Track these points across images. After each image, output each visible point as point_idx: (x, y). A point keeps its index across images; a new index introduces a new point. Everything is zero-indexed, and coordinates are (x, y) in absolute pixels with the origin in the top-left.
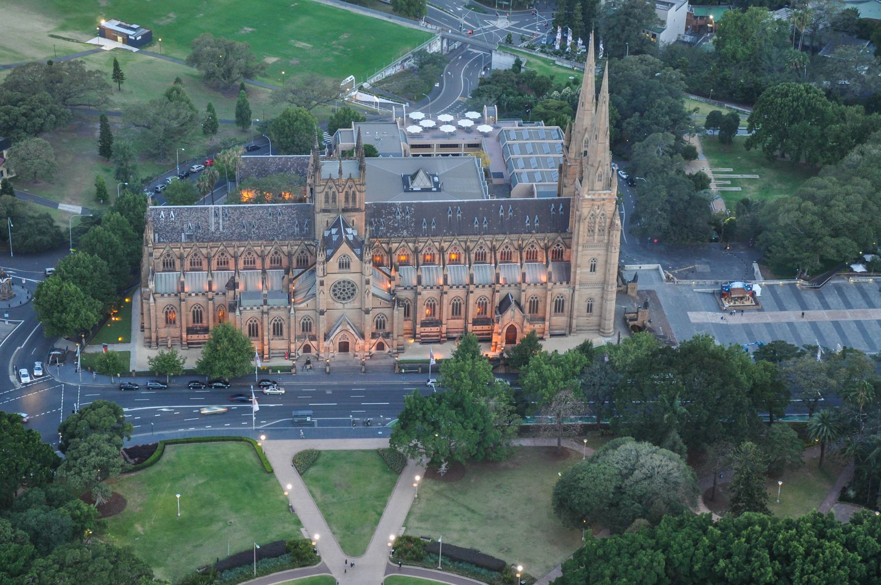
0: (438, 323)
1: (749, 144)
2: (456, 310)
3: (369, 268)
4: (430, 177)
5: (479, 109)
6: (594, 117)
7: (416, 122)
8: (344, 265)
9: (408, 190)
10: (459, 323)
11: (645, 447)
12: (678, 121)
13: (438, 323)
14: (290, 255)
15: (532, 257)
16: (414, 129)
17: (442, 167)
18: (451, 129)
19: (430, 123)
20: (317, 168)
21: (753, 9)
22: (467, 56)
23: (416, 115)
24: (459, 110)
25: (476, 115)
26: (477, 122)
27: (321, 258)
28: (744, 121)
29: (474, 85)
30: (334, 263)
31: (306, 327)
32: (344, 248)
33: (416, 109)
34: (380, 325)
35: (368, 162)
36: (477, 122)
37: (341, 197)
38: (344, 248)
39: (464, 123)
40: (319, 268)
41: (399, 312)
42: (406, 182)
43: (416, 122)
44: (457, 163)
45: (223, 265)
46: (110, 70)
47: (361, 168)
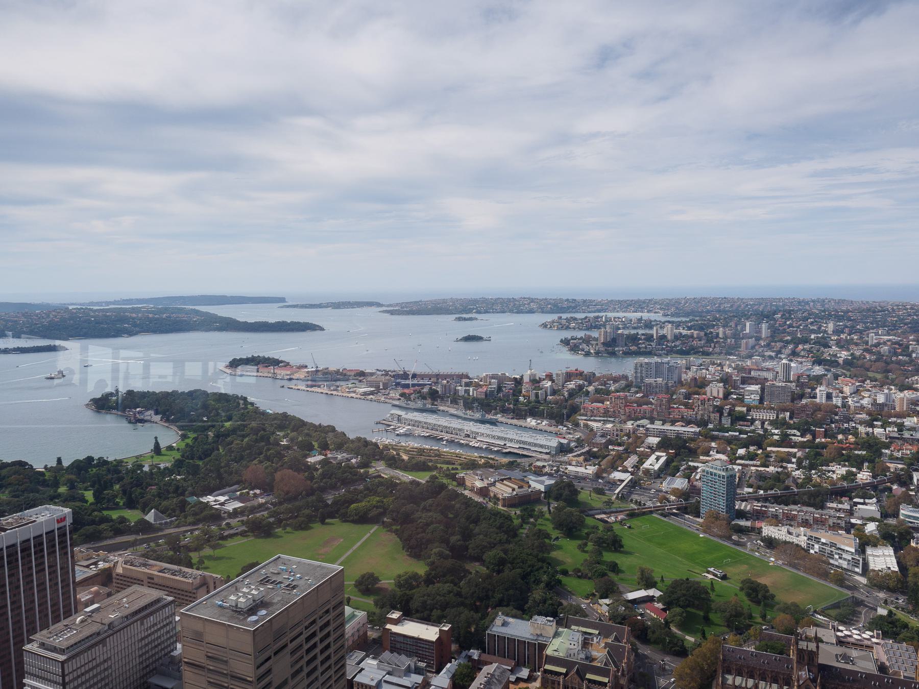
7: (842, 631)
16: (839, 634)
17: (854, 653)
18: (859, 638)
20: (797, 644)
24: (861, 630)
26: (872, 637)
29: (868, 620)
35: (820, 644)
36: (872, 637)
43: (842, 631)
45: (752, 677)
46: (709, 586)
47: (818, 647)
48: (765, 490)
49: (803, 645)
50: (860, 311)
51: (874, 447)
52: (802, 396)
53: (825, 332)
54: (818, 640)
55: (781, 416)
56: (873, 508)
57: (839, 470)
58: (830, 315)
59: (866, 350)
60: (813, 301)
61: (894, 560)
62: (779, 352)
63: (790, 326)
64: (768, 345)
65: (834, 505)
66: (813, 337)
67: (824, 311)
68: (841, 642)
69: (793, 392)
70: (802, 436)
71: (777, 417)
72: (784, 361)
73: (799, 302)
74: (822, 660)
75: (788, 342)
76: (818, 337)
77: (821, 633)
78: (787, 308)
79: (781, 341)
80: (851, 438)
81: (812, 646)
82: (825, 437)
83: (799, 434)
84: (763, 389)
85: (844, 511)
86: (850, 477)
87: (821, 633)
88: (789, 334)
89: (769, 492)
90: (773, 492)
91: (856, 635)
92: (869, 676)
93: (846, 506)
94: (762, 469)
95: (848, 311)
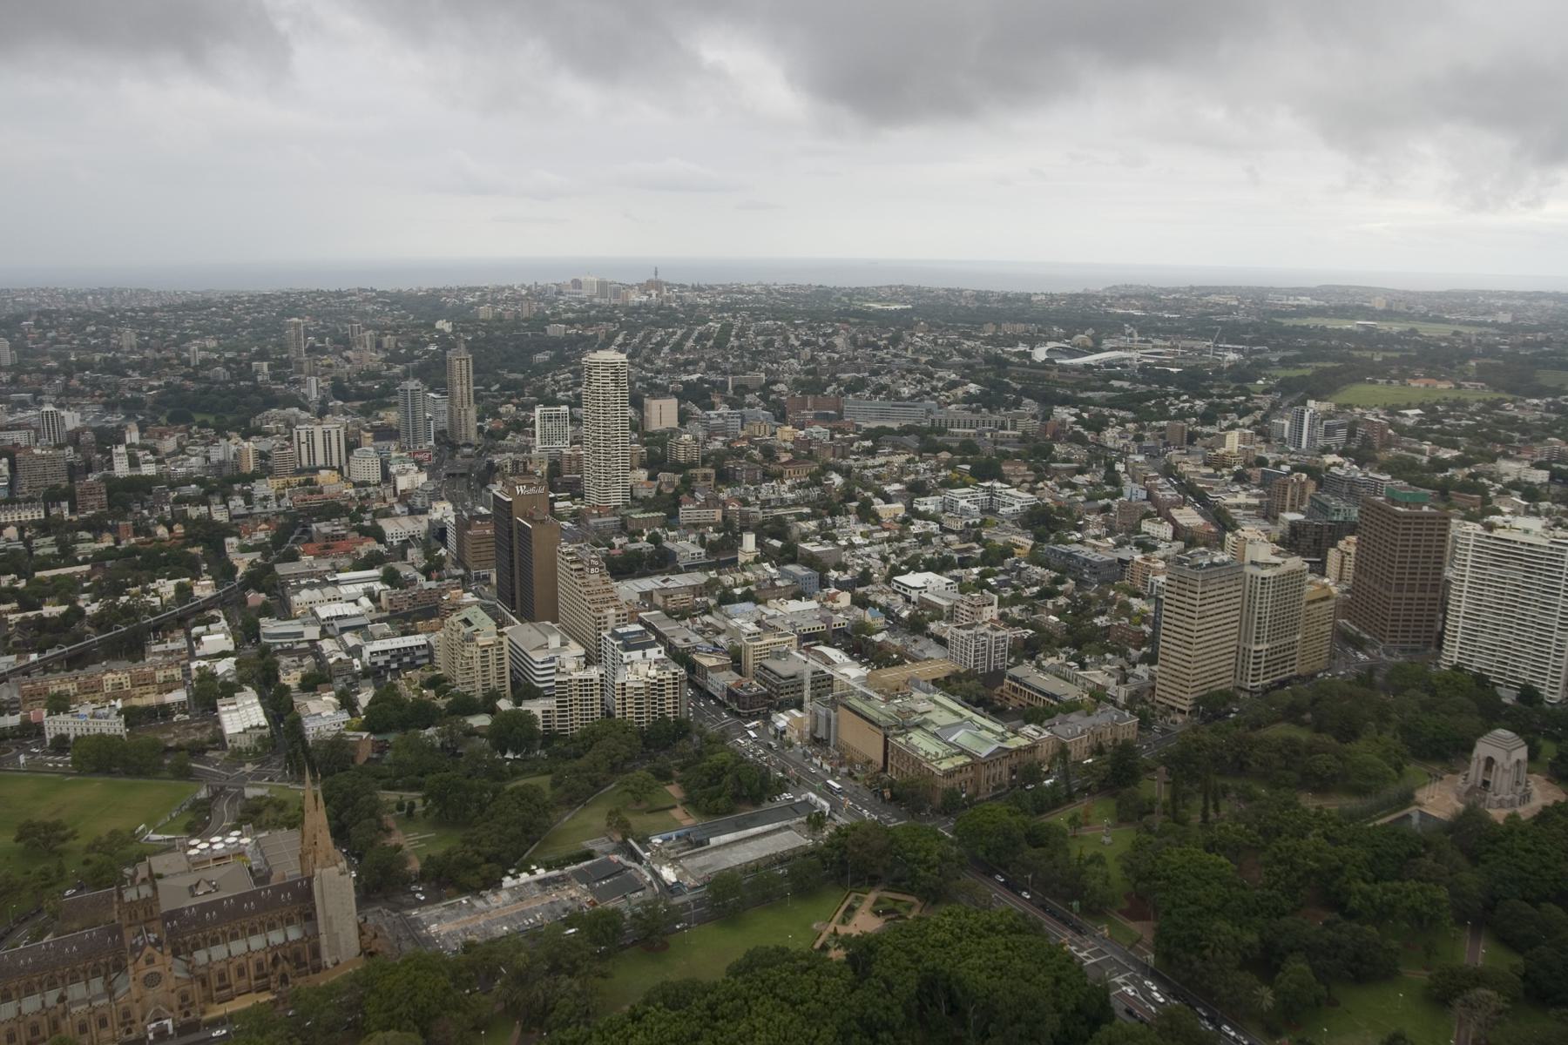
0: (229, 986)
1: (425, 814)
2: (241, 972)
3: (169, 959)
4: (209, 883)
5: (239, 829)
6: (318, 819)
7: (194, 847)
8: (150, 961)
9: (193, 896)
10: (244, 981)
11: (392, 1033)
12: (375, 810)
13: (229, 986)
14: (107, 964)
15: (290, 922)
16: (192, 852)
17: (215, 874)
19: (205, 845)
20: (121, 896)
21: (411, 731)
22: (227, 794)
23: (194, 842)
24: (225, 833)
25: (237, 833)
27: (130, 961)
28: (419, 802)
30: (142, 961)
31: (126, 1014)
32: (149, 949)
33: (193, 837)
34: (184, 998)
35: (159, 882)
36: (241, 836)
37: (141, 913)
38: (149, 949)
39: (230, 840)
40: (130, 968)
41: (197, 986)
42: (192, 890)
43: (194, 847)
44: (227, 869)
47: (155, 888)
48: (41, 651)
49: (131, 895)
50: (172, 308)
51: (212, 535)
52: (89, 469)
53: (118, 349)
54: (153, 878)
55: (54, 511)
56: (222, 636)
57: (167, 587)
58: (123, 317)
59: (186, 376)
60: (92, 292)
61: (259, 709)
62: (38, 392)
63: (55, 341)
64: (14, 381)
65: (161, 647)
66: (97, 357)
67: (112, 311)
68: (199, 863)
69: (71, 466)
70: (95, 540)
71: (47, 514)
72: (48, 408)
73: (67, 295)
74: (166, 905)
75: (51, 373)
76: (106, 359)
77: (159, 863)
78: (45, 306)
79: (39, 370)
80: (179, 529)
81: (146, 891)
82: (136, 534)
83: (89, 536)
84: (13, 466)
85: (179, 652)
86: (184, 593)
87: (159, 863)
88: (56, 357)
89: (49, 654)
90: (56, 651)
91: (218, 844)
92: (240, 899)
93: (181, 644)
94: (30, 614)
95: (153, 310)
